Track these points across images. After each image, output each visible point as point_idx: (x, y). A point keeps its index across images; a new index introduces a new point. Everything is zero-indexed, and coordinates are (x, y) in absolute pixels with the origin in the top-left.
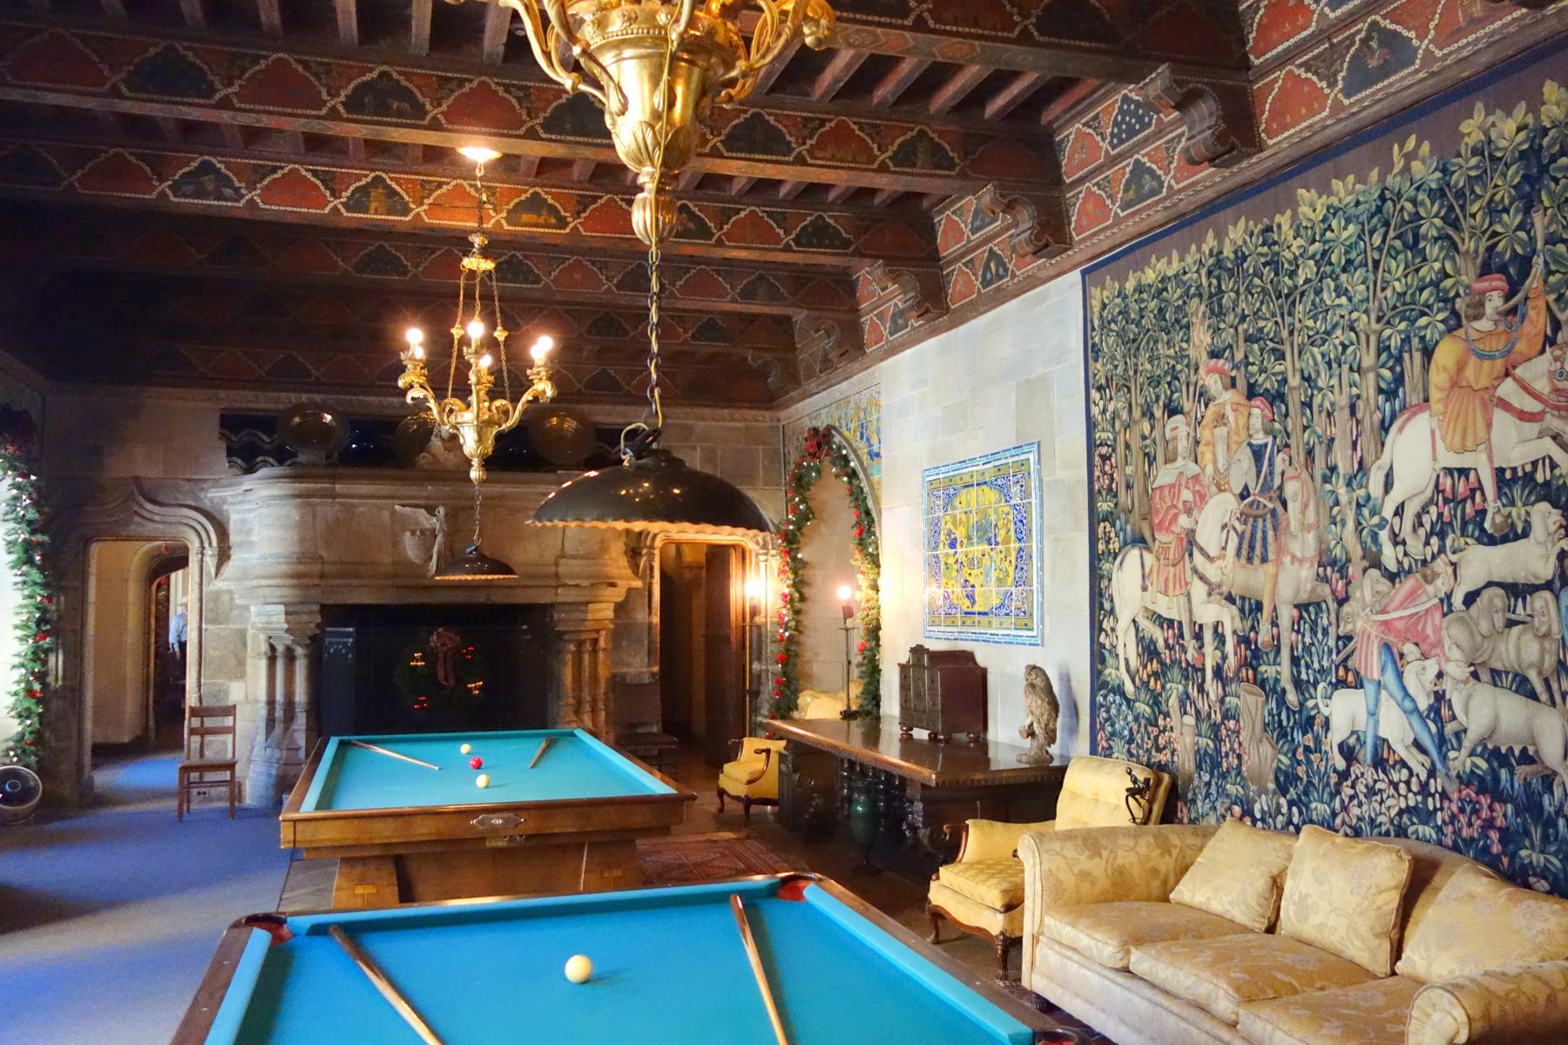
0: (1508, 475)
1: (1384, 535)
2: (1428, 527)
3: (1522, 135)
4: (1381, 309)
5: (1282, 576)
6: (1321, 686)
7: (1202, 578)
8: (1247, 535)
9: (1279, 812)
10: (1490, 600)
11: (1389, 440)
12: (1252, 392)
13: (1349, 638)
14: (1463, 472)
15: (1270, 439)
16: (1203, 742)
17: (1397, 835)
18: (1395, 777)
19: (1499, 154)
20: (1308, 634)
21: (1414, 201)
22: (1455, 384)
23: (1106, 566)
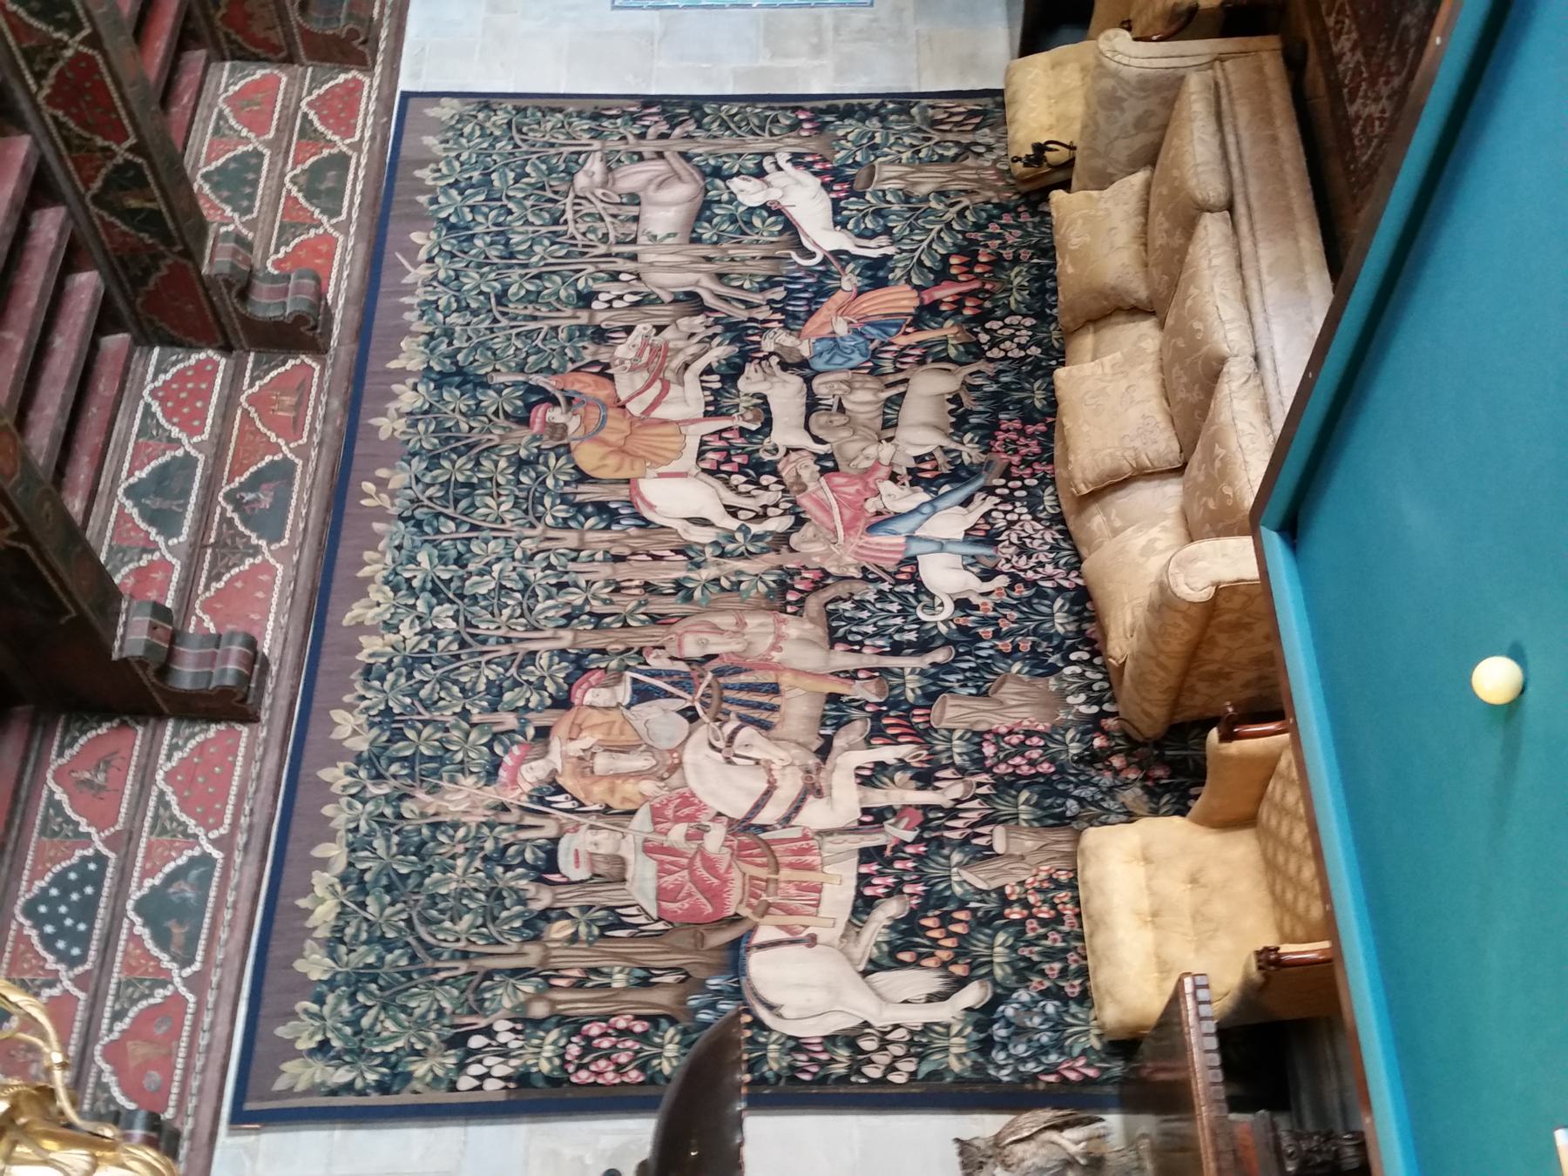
0: (711, 408)
1: (755, 529)
2: (751, 487)
3: (421, 388)
4: (522, 526)
5: (796, 664)
6: (923, 617)
7: (797, 808)
8: (743, 711)
9: (1082, 676)
10: (821, 427)
11: (659, 520)
12: (562, 703)
13: (864, 569)
14: (702, 443)
15: (629, 674)
16: (1025, 813)
17: (1063, 522)
18: (1001, 524)
19: (426, 406)
20: (864, 629)
21: (428, 486)
22: (622, 451)
23: (775, 1061)
